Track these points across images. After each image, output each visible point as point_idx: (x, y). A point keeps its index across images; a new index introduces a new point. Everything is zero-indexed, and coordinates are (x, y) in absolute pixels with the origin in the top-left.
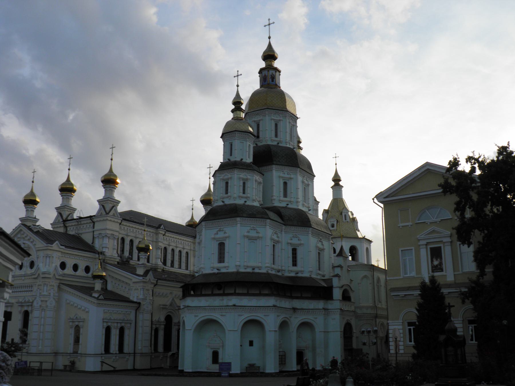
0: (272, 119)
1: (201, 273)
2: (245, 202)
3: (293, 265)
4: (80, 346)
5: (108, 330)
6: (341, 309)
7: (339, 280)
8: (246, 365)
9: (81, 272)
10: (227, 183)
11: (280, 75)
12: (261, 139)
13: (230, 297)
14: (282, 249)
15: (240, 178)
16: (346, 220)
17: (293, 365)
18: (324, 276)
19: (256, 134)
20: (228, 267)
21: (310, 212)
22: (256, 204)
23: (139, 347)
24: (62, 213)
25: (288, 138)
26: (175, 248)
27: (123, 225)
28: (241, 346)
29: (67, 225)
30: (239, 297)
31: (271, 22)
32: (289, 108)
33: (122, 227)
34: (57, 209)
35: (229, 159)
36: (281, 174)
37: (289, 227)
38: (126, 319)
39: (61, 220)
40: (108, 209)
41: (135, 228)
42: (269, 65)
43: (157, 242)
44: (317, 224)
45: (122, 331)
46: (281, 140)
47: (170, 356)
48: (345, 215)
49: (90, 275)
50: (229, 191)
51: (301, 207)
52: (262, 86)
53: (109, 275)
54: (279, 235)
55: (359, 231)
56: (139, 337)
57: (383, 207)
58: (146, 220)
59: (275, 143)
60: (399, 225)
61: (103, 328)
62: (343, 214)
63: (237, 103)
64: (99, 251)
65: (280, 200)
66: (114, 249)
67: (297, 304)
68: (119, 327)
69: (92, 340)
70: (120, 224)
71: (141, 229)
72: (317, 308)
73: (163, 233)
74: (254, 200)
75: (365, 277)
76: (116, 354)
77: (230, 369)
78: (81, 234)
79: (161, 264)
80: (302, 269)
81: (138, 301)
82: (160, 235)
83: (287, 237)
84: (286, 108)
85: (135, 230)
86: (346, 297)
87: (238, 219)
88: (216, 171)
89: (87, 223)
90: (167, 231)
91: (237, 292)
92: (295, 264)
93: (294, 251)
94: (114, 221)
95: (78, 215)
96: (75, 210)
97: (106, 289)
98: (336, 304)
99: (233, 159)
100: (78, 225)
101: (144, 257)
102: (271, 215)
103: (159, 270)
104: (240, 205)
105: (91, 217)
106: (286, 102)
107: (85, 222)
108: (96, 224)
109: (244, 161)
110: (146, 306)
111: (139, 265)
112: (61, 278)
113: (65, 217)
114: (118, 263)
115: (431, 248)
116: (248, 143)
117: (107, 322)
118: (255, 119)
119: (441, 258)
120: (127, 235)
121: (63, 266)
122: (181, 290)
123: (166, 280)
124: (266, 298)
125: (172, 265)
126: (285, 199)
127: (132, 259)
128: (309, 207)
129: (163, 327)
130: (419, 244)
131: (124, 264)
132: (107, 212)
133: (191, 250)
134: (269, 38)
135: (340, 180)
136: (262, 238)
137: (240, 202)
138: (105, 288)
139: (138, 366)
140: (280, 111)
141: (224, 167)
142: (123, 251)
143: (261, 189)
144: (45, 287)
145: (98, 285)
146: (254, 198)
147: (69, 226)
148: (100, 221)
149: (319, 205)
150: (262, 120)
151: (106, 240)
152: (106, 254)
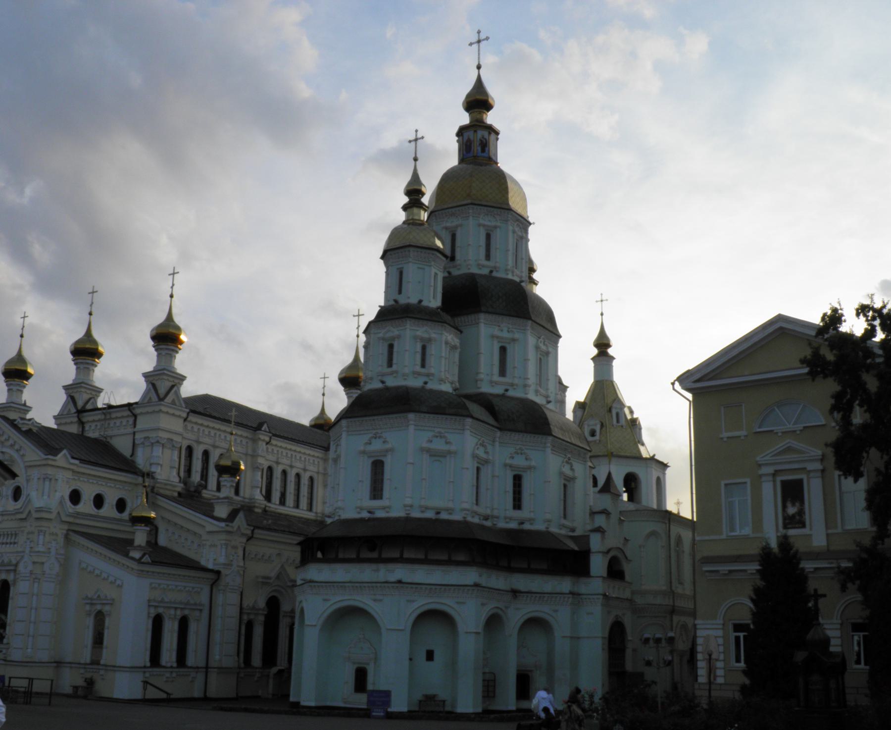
0: (479, 225)
1: (337, 518)
2: (426, 383)
4: (104, 651)
5: (158, 623)
6: (605, 595)
7: (603, 538)
8: (419, 696)
9: (109, 509)
10: (391, 347)
11: (497, 139)
12: (458, 262)
13: (391, 566)
14: (493, 476)
15: (415, 338)
16: (618, 421)
17: (508, 701)
18: (573, 530)
19: (448, 252)
20: (389, 507)
21: (550, 406)
22: (446, 388)
23: (216, 656)
24: (76, 396)
25: (511, 263)
26: (288, 469)
27: (190, 422)
28: (411, 659)
29: (84, 420)
30: (409, 566)
32: (514, 203)
33: (189, 426)
34: (66, 388)
35: (396, 301)
36: (497, 332)
37: (509, 433)
38: (192, 602)
39: (73, 410)
40: (162, 392)
41: (213, 428)
42: (477, 121)
43: (254, 456)
44: (562, 429)
45: (184, 624)
46: (498, 265)
47: (275, 675)
48: (617, 414)
49: (125, 515)
50: (395, 361)
51: (532, 396)
52: (462, 160)
53: (163, 518)
54: (489, 448)
55: (643, 444)
56: (217, 637)
57: (691, 399)
58: (234, 413)
59: (485, 271)
61: (149, 617)
62: (614, 412)
63: (414, 192)
64: (145, 470)
65: (491, 382)
66: (172, 467)
67: (521, 582)
68: (179, 617)
69: (128, 641)
70: (185, 420)
71: (225, 431)
72: (558, 590)
73: (267, 439)
74: (441, 381)
75: (653, 534)
76: (172, 667)
77: (388, 703)
78: (111, 437)
79: (262, 498)
80: (532, 515)
81: (216, 568)
82: (260, 443)
83: (505, 452)
84: (508, 204)
85: (213, 432)
86: (615, 572)
87: (411, 416)
88: (370, 323)
89: (123, 417)
90: (275, 435)
91: (406, 555)
92: (517, 504)
93: (517, 480)
94: (173, 415)
95: (106, 402)
96: (99, 391)
97: (156, 543)
98: (596, 583)
99: (403, 300)
100: (105, 419)
101: (228, 485)
102: (475, 409)
103: (257, 510)
104: (415, 389)
105: (129, 405)
106: (507, 192)
107: (119, 415)
108: (140, 420)
109: (424, 303)
110: (231, 578)
111: (219, 498)
112: (71, 520)
113: (80, 404)
114: (179, 494)
116: (434, 270)
117: (156, 607)
118: (449, 225)
120: (198, 442)
121: (75, 497)
122: (299, 549)
123: (269, 529)
124: (461, 569)
125: (283, 502)
126: (502, 379)
127: (205, 487)
128: (547, 397)
129: (261, 618)
131: (191, 496)
132: (162, 396)
133: (318, 473)
135: (608, 345)
136: (455, 453)
137: (415, 383)
138: (153, 541)
139: (212, 693)
140: (495, 210)
141: (385, 315)
142: (189, 471)
143: (457, 359)
144: (41, 537)
145: (141, 537)
146: (443, 378)
147: (88, 422)
148: (148, 413)
149: (567, 394)
150: (461, 225)
151: (158, 451)
152: (157, 476)
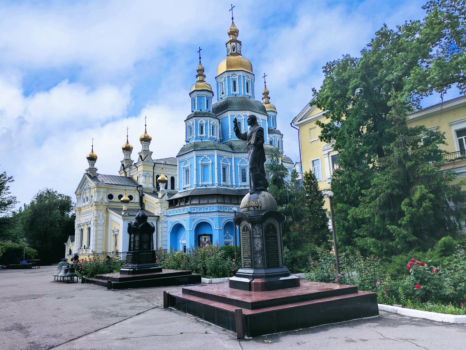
3: (243, 181)
11: (241, 45)
31: (233, 6)
40: (143, 158)
105: (135, 164)
121: (110, 197)
134: (233, 19)
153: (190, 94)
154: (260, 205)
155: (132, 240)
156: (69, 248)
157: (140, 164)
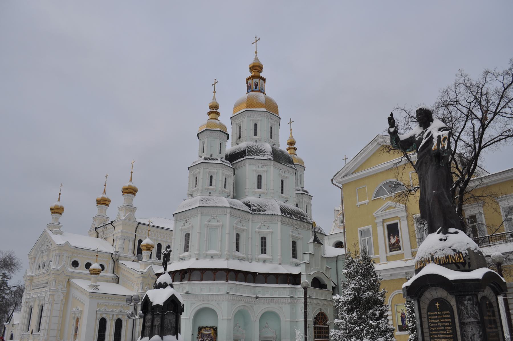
5: (103, 323)
11: (265, 83)
31: (257, 39)
36: (254, 168)
45: (119, 323)
60: (356, 205)
105: (112, 222)
115: (388, 226)
119: (398, 235)
130: (376, 221)
153: (198, 135)
154: (467, 261)
155: (148, 324)
156: (10, 331)
157: (119, 223)
